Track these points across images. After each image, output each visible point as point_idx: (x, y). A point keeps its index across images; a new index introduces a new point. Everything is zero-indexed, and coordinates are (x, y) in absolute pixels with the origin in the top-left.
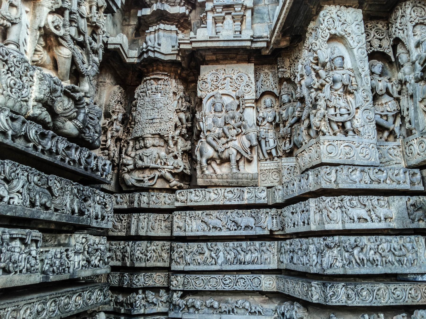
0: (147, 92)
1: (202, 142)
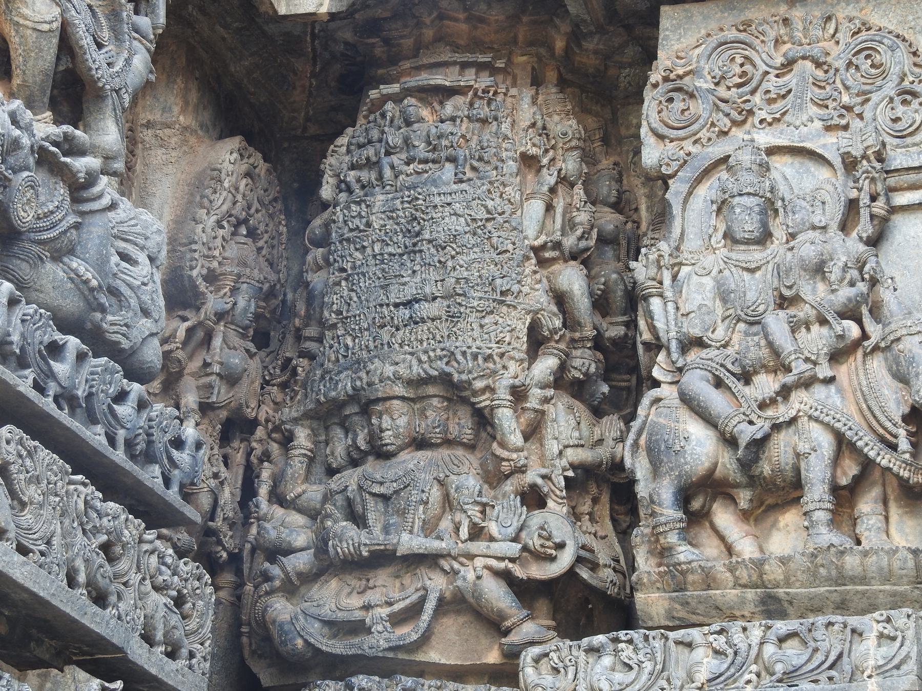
0: (385, 161)
1: (658, 400)
